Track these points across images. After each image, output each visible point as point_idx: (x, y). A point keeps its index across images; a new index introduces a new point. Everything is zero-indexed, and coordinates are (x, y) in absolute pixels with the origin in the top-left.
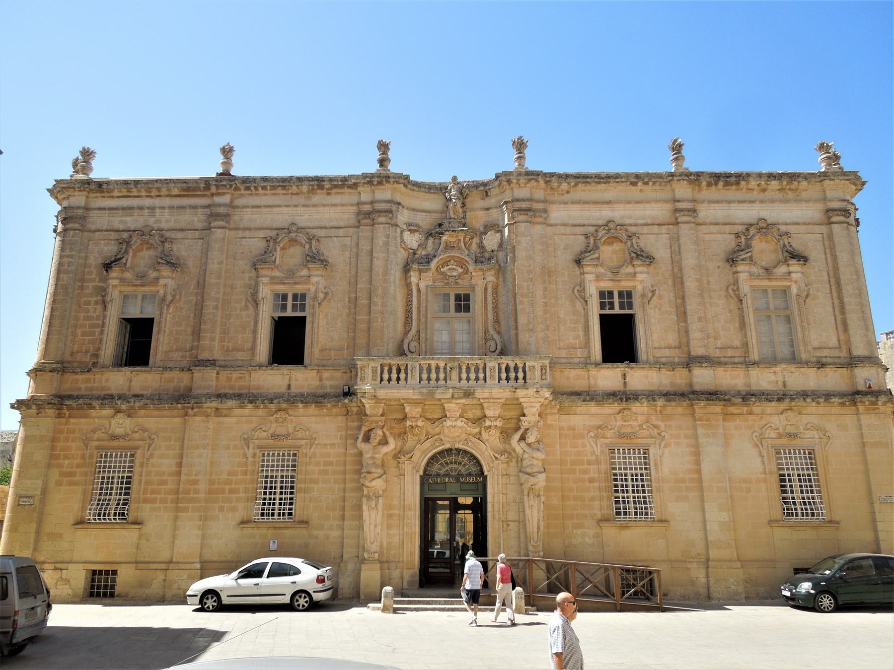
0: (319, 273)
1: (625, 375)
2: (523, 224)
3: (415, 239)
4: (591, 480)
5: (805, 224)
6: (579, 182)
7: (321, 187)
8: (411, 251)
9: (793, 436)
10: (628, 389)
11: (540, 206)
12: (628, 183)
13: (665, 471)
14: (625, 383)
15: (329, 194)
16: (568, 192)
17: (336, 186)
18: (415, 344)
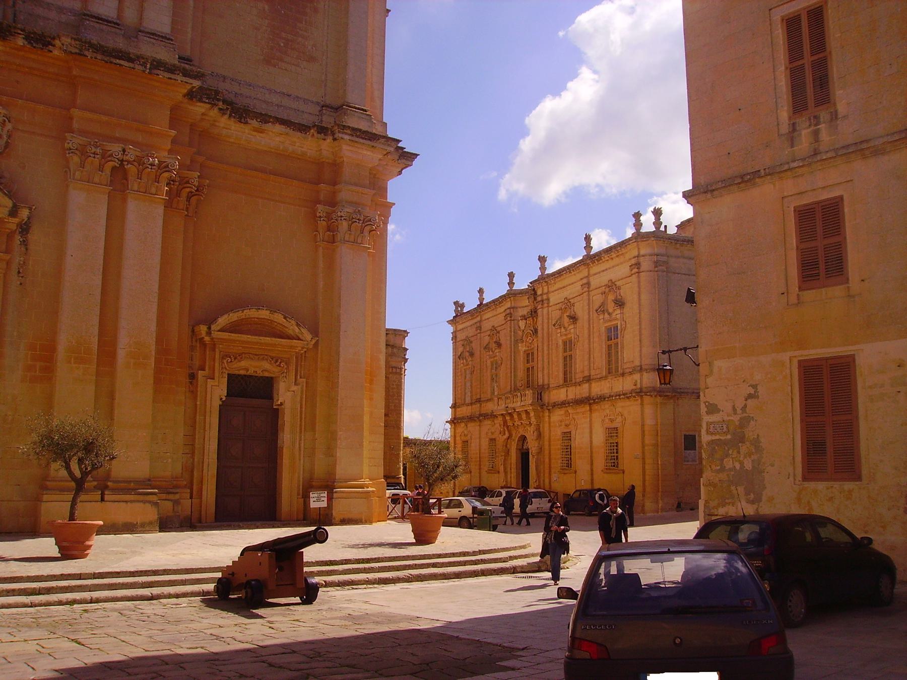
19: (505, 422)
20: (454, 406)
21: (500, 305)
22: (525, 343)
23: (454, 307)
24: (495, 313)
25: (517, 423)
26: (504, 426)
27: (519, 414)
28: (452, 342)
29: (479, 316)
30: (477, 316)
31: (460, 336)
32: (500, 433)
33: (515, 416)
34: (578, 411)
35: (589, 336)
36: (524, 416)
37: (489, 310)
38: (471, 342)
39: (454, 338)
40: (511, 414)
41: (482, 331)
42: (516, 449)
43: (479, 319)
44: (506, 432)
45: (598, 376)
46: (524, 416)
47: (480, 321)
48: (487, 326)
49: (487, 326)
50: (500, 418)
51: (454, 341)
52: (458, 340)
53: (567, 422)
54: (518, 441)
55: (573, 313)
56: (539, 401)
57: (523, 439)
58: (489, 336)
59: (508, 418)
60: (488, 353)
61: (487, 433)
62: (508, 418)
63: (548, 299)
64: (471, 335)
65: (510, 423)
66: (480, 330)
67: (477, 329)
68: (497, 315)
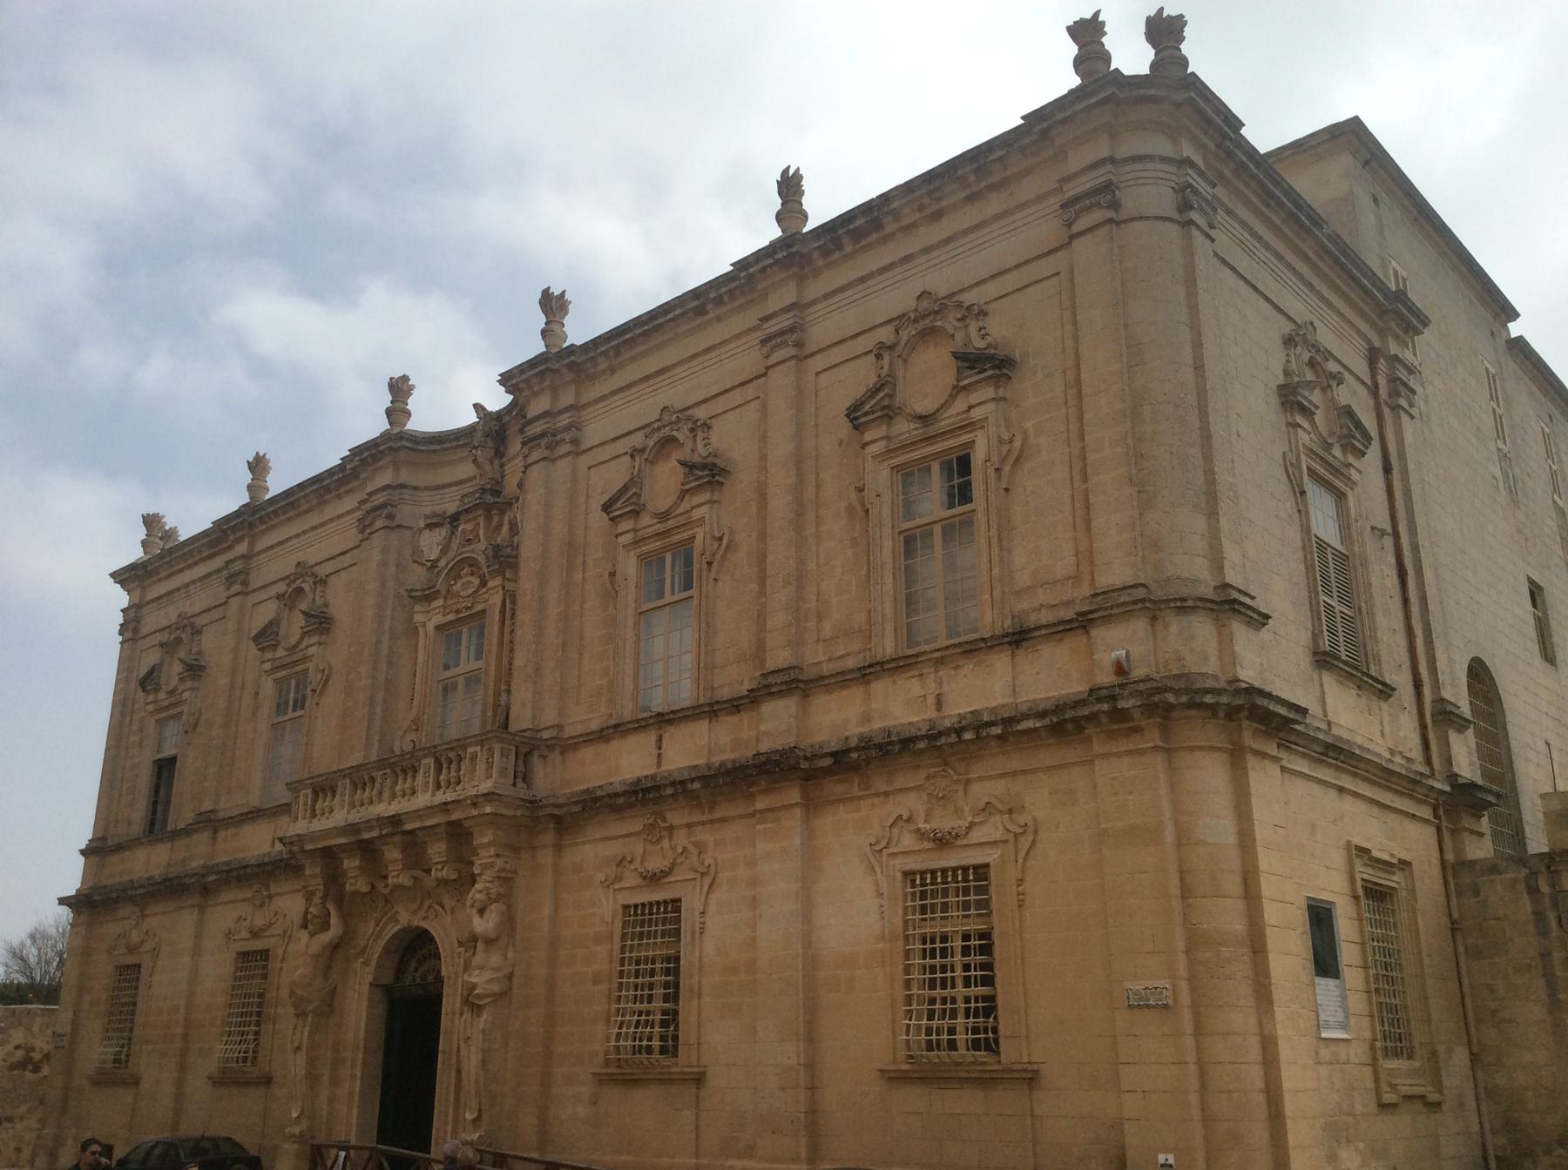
0: (315, 639)
1: (660, 739)
2: (536, 466)
3: (435, 540)
4: (596, 980)
5: (1017, 266)
6: (618, 346)
7: (327, 489)
8: (429, 564)
9: (942, 842)
10: (663, 768)
11: (564, 420)
12: (692, 314)
13: (710, 945)
14: (659, 755)
15: (339, 497)
16: (613, 371)
17: (341, 482)
18: (414, 738)
19: (334, 879)
20: (95, 851)
21: (342, 490)
22: (440, 602)
23: (142, 532)
24: (314, 519)
25: (399, 877)
26: (324, 898)
27: (413, 844)
28: (120, 639)
29: (246, 540)
30: (239, 540)
31: (154, 620)
32: (304, 926)
33: (392, 854)
34: (719, 813)
35: (799, 514)
36: (437, 850)
37: (292, 513)
38: (197, 632)
39: (131, 626)
40: (368, 851)
41: (250, 589)
42: (371, 984)
43: (241, 549)
44: (334, 920)
45: (851, 663)
46: (437, 850)
47: (246, 557)
48: (274, 568)
49: (274, 568)
50: (313, 870)
51: (129, 634)
52: (145, 630)
53: (656, 864)
54: (387, 950)
55: (701, 450)
56: (520, 784)
57: (417, 945)
58: (279, 597)
59: (351, 864)
60: (269, 655)
61: (229, 935)
62: (351, 864)
63: (575, 426)
64: (198, 608)
65: (357, 883)
66: (245, 583)
67: (230, 580)
68: (322, 525)
